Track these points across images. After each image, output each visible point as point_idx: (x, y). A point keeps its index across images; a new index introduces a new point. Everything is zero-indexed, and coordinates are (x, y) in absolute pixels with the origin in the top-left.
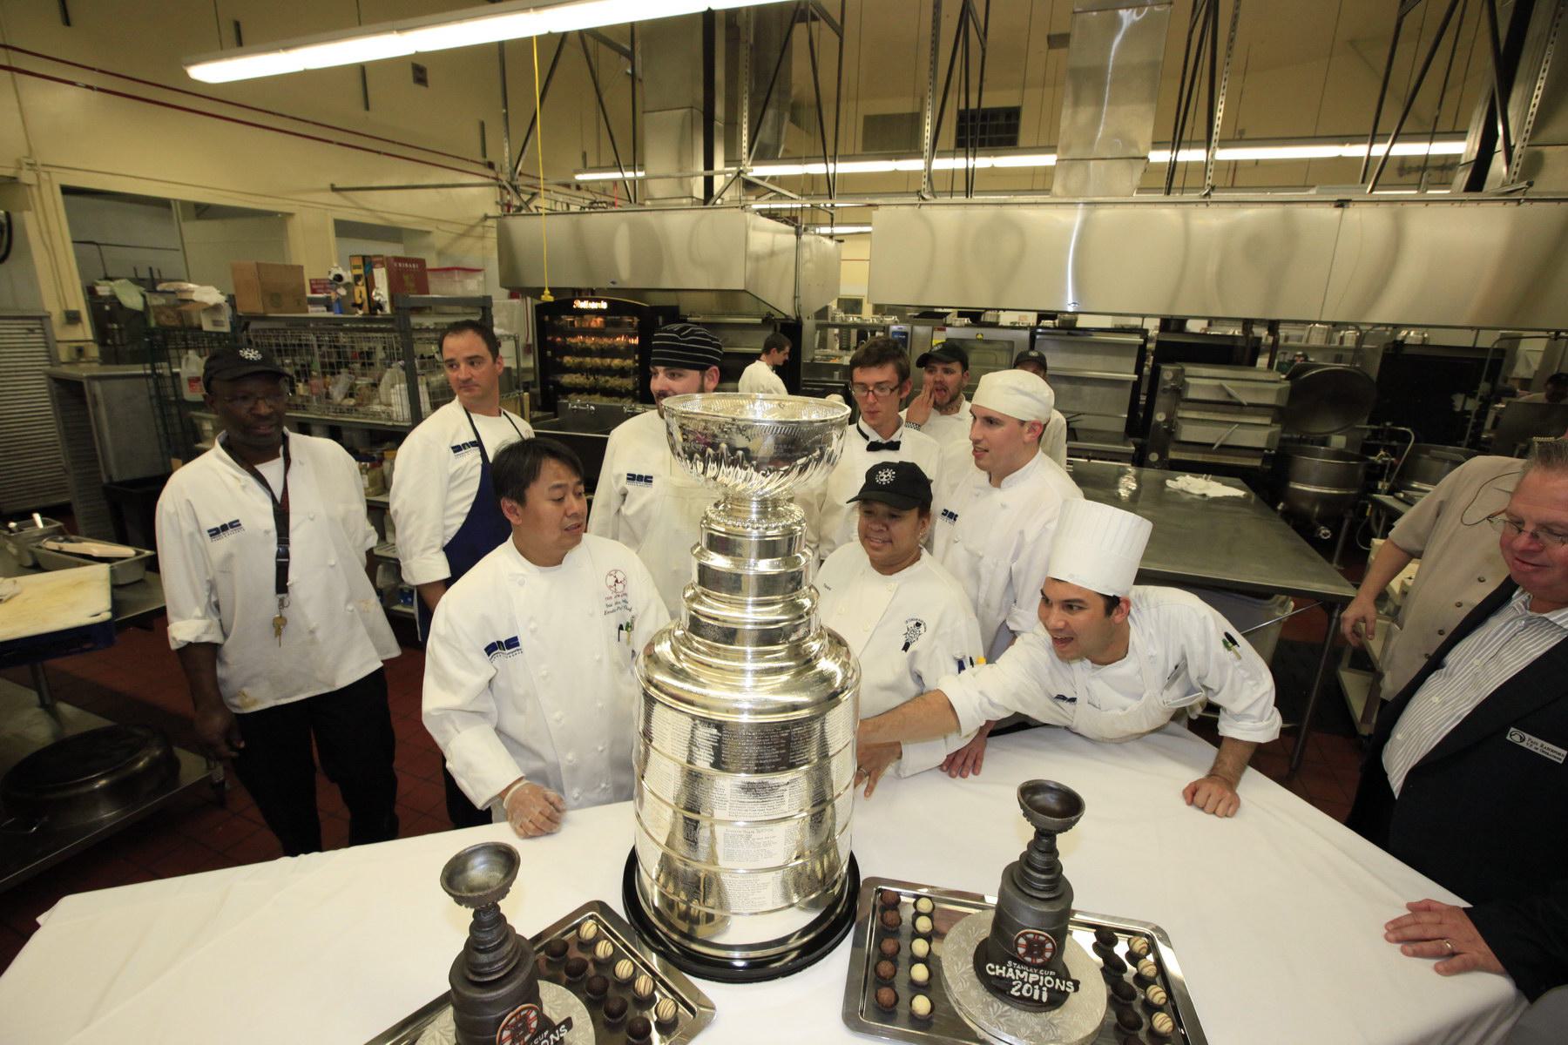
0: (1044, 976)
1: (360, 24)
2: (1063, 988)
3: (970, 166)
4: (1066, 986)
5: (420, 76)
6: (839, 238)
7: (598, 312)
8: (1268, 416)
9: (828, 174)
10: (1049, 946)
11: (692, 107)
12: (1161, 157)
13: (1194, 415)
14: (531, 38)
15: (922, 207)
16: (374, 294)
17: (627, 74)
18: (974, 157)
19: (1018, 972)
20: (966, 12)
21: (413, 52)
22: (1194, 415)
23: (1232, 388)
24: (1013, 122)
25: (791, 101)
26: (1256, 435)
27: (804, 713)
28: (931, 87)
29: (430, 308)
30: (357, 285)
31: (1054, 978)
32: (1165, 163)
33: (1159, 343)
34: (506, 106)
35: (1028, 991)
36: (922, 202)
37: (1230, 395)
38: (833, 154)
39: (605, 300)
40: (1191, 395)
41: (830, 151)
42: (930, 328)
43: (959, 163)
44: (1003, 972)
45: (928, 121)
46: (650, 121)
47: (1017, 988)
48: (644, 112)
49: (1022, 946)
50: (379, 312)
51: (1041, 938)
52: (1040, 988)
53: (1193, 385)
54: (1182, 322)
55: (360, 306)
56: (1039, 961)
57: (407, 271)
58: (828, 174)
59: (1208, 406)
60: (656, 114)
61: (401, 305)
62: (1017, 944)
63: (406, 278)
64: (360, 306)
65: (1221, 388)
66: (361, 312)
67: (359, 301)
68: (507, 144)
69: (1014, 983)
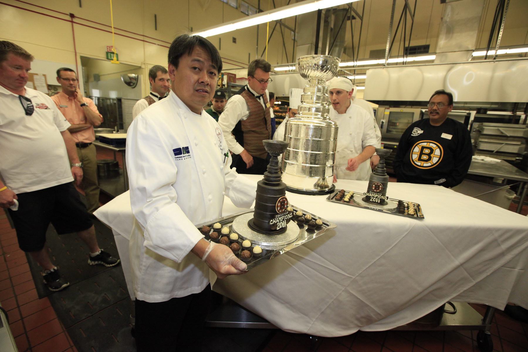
0: (379, 195)
1: (223, 22)
2: (384, 199)
3: (405, 61)
4: (385, 198)
5: (235, 41)
6: (357, 85)
7: (278, 105)
8: (520, 141)
9: (354, 65)
10: (381, 187)
11: (312, 44)
12: (483, 53)
13: (486, 140)
14: (267, 23)
15: (384, 69)
16: (223, 82)
17: (292, 39)
18: (407, 58)
19: (372, 194)
20: (406, 6)
21: (236, 29)
22: (486, 140)
23: (502, 129)
24: (427, 50)
25: (345, 45)
26: (513, 148)
27: (324, 125)
28: (390, 30)
29: (236, 87)
30: (219, 80)
31: (382, 195)
32: (483, 56)
33: (475, 118)
34: (257, 45)
35: (375, 200)
36: (384, 67)
37: (502, 133)
38: (356, 59)
39: (280, 101)
40: (485, 132)
41: (355, 58)
42: (384, 108)
43: (400, 60)
44: (368, 194)
45: (388, 41)
46: (298, 49)
47: (372, 199)
48: (297, 46)
49: (374, 187)
50: (224, 87)
51: (379, 184)
52: (378, 199)
53: (487, 129)
54: (486, 110)
55: (219, 86)
56: (378, 191)
57: (232, 77)
58: (354, 65)
59: (493, 137)
60: (301, 46)
61: (229, 85)
62: (372, 187)
63: (231, 78)
64: (219, 86)
65: (499, 130)
66: (219, 87)
67: (219, 84)
68: (257, 56)
69: (371, 198)
